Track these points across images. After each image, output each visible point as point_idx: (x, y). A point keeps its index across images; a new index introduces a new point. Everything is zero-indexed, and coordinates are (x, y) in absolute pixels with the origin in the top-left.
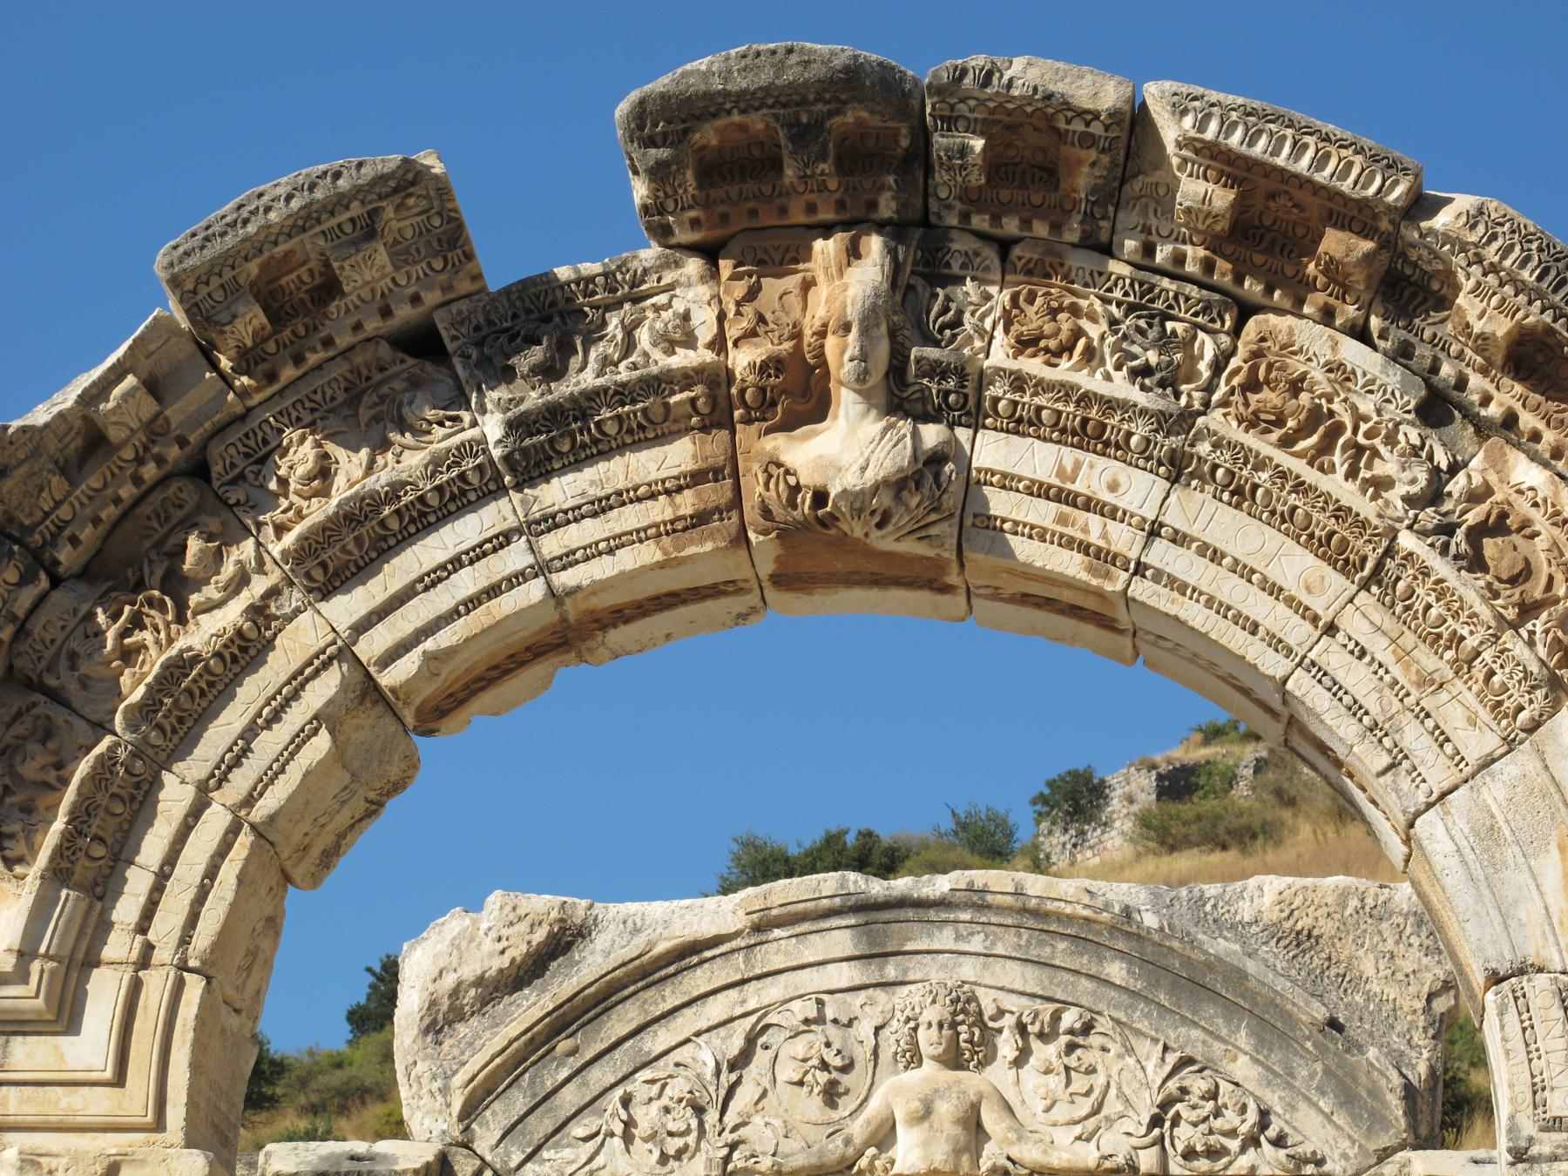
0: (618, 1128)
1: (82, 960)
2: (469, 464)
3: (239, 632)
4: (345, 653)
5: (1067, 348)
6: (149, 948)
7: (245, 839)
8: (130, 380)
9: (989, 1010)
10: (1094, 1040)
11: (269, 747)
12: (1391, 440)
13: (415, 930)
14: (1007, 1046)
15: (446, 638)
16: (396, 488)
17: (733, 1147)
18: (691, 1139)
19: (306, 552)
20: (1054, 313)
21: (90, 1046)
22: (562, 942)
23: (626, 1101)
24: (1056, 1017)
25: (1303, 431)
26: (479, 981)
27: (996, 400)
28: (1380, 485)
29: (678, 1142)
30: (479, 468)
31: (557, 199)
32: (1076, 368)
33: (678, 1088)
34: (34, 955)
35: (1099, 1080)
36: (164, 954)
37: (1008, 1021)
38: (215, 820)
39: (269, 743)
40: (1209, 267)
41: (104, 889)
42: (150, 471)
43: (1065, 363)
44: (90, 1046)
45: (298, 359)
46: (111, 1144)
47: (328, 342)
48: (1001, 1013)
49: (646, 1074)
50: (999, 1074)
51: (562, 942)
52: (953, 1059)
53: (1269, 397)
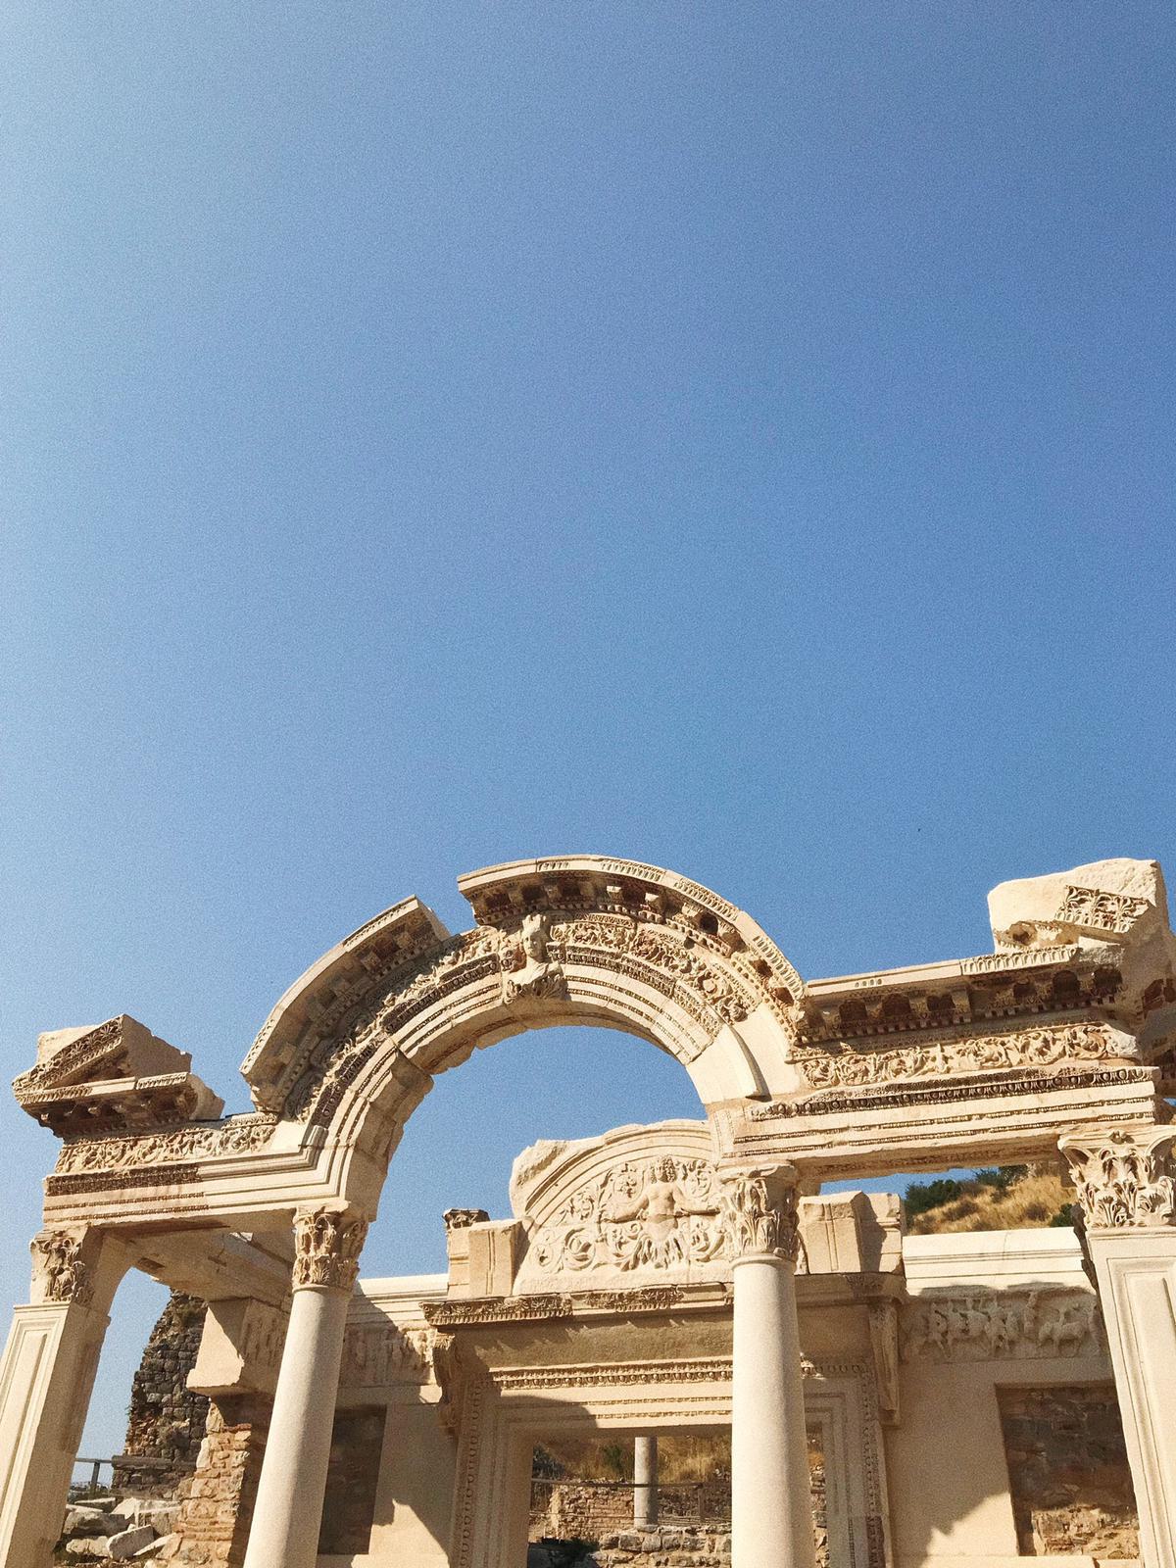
0: (570, 1210)
1: (318, 1148)
2: (431, 992)
3: (368, 1047)
4: (397, 1050)
5: (589, 938)
6: (338, 1141)
7: (368, 1106)
9: (675, 1163)
10: (706, 1169)
11: (374, 1081)
12: (678, 954)
13: (517, 1153)
14: (680, 1174)
15: (425, 1042)
16: (410, 1001)
17: (602, 1212)
18: (590, 1211)
20: (586, 929)
22: (554, 1154)
23: (572, 1201)
24: (694, 1163)
25: (654, 954)
26: (533, 1168)
27: (569, 956)
28: (675, 967)
29: (586, 1212)
30: (433, 992)
31: (456, 918)
32: (592, 944)
33: (586, 1195)
34: (306, 1147)
35: (708, 1182)
36: (343, 1143)
37: (681, 1165)
38: (360, 1101)
39: (376, 1078)
40: (621, 909)
41: (327, 1122)
42: (349, 1004)
43: (589, 942)
45: (389, 968)
47: (397, 963)
48: (679, 1163)
49: (577, 1192)
50: (679, 1182)
51: (554, 1154)
52: (665, 1179)
53: (643, 948)
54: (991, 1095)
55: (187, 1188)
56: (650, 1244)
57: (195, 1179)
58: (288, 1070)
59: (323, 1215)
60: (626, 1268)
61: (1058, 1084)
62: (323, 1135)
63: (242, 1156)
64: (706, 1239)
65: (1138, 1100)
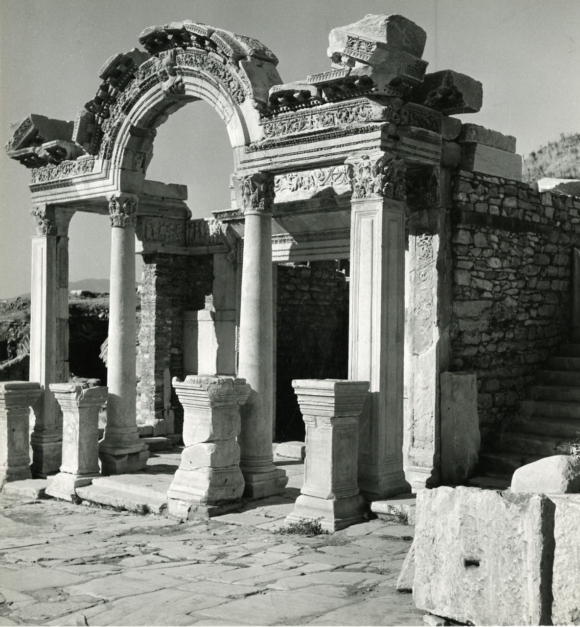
1: (107, 170)
8: (101, 91)
11: (124, 137)
15: (140, 118)
19: (123, 108)
21: (110, 181)
39: (124, 136)
41: (110, 158)
44: (110, 181)
46: (112, 193)
54: (324, 139)
55: (71, 187)
56: (302, 178)
57: (72, 185)
58: (93, 135)
59: (113, 199)
60: (293, 190)
61: (347, 133)
62: (109, 164)
63: (85, 174)
64: (324, 175)
65: (374, 140)
